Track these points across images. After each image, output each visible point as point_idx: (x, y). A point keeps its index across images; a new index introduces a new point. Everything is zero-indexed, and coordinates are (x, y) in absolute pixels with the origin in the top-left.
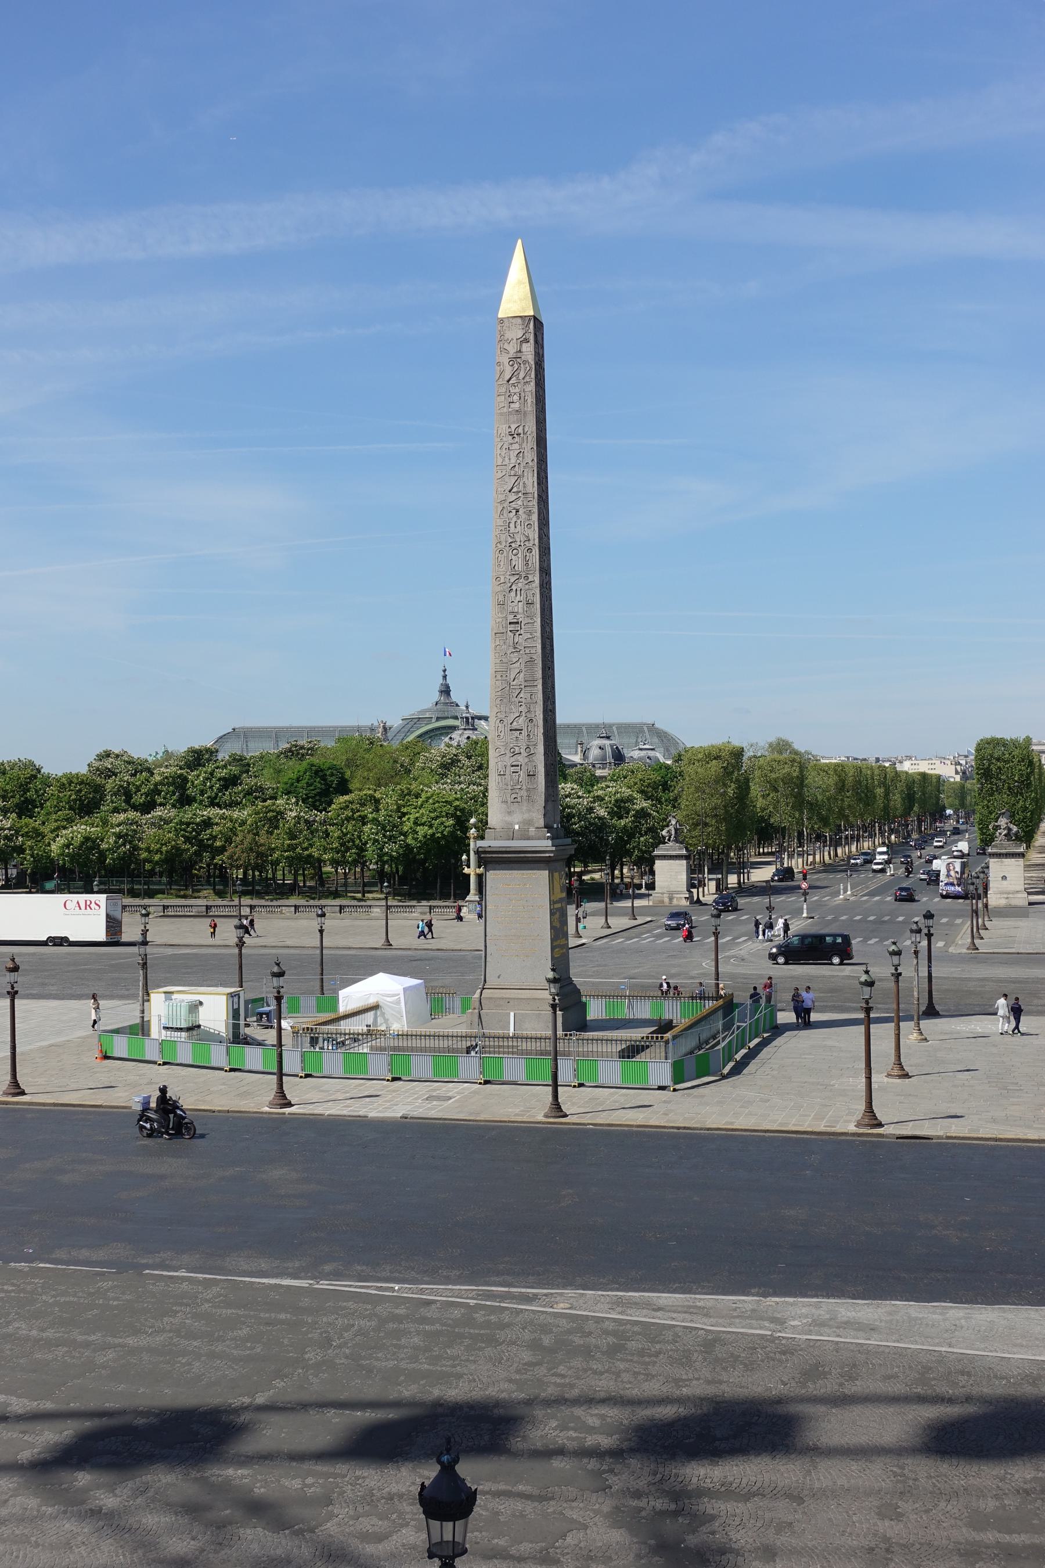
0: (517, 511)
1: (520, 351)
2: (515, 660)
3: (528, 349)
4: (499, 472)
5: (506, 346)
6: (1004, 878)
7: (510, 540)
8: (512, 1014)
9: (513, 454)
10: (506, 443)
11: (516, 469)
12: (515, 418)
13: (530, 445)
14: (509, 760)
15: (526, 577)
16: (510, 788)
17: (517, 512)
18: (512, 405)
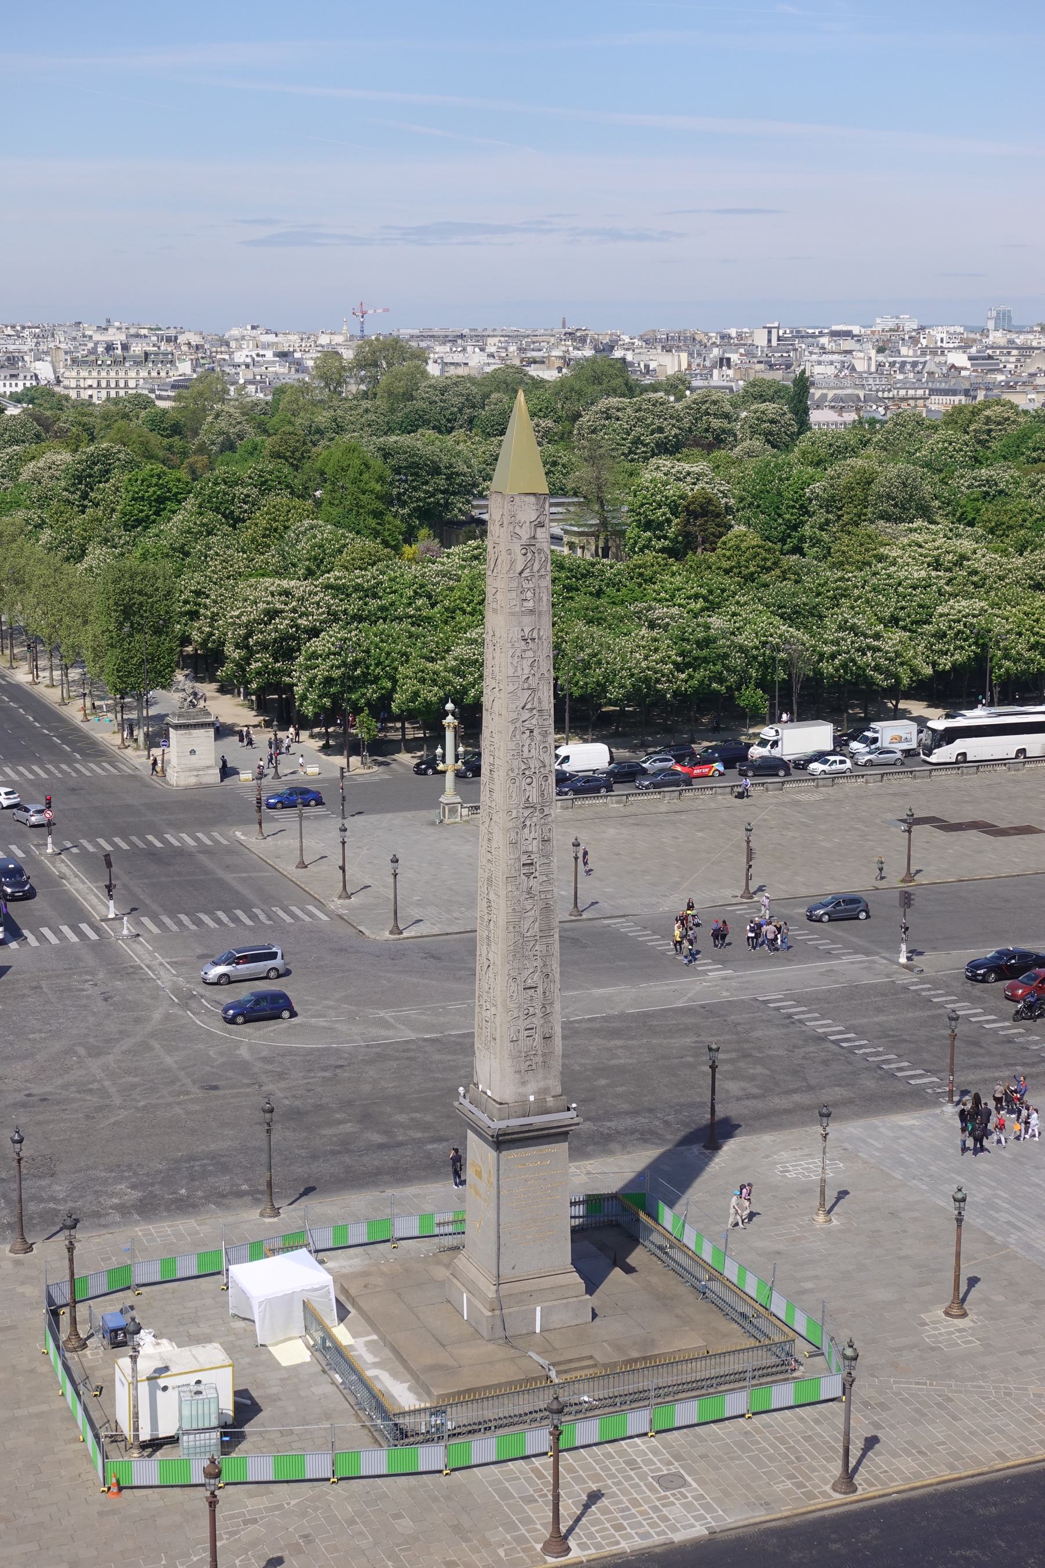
0: (532, 731)
1: (534, 537)
2: (529, 908)
3: (544, 535)
4: (511, 684)
5: (518, 530)
6: (193, 752)
7: (523, 767)
8: (538, 1309)
9: (526, 664)
10: (519, 650)
11: (530, 681)
12: (527, 620)
13: (545, 653)
14: (522, 1024)
15: (542, 810)
16: (524, 1054)
17: (532, 731)
18: (525, 604)
